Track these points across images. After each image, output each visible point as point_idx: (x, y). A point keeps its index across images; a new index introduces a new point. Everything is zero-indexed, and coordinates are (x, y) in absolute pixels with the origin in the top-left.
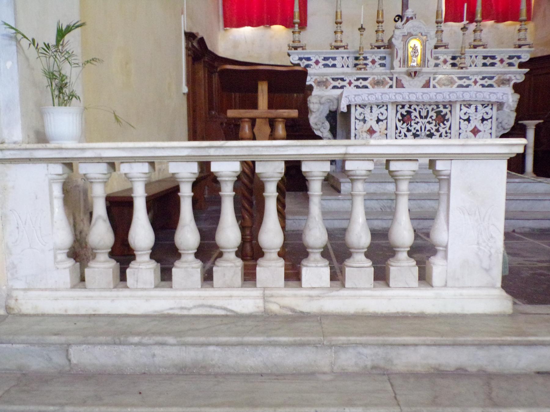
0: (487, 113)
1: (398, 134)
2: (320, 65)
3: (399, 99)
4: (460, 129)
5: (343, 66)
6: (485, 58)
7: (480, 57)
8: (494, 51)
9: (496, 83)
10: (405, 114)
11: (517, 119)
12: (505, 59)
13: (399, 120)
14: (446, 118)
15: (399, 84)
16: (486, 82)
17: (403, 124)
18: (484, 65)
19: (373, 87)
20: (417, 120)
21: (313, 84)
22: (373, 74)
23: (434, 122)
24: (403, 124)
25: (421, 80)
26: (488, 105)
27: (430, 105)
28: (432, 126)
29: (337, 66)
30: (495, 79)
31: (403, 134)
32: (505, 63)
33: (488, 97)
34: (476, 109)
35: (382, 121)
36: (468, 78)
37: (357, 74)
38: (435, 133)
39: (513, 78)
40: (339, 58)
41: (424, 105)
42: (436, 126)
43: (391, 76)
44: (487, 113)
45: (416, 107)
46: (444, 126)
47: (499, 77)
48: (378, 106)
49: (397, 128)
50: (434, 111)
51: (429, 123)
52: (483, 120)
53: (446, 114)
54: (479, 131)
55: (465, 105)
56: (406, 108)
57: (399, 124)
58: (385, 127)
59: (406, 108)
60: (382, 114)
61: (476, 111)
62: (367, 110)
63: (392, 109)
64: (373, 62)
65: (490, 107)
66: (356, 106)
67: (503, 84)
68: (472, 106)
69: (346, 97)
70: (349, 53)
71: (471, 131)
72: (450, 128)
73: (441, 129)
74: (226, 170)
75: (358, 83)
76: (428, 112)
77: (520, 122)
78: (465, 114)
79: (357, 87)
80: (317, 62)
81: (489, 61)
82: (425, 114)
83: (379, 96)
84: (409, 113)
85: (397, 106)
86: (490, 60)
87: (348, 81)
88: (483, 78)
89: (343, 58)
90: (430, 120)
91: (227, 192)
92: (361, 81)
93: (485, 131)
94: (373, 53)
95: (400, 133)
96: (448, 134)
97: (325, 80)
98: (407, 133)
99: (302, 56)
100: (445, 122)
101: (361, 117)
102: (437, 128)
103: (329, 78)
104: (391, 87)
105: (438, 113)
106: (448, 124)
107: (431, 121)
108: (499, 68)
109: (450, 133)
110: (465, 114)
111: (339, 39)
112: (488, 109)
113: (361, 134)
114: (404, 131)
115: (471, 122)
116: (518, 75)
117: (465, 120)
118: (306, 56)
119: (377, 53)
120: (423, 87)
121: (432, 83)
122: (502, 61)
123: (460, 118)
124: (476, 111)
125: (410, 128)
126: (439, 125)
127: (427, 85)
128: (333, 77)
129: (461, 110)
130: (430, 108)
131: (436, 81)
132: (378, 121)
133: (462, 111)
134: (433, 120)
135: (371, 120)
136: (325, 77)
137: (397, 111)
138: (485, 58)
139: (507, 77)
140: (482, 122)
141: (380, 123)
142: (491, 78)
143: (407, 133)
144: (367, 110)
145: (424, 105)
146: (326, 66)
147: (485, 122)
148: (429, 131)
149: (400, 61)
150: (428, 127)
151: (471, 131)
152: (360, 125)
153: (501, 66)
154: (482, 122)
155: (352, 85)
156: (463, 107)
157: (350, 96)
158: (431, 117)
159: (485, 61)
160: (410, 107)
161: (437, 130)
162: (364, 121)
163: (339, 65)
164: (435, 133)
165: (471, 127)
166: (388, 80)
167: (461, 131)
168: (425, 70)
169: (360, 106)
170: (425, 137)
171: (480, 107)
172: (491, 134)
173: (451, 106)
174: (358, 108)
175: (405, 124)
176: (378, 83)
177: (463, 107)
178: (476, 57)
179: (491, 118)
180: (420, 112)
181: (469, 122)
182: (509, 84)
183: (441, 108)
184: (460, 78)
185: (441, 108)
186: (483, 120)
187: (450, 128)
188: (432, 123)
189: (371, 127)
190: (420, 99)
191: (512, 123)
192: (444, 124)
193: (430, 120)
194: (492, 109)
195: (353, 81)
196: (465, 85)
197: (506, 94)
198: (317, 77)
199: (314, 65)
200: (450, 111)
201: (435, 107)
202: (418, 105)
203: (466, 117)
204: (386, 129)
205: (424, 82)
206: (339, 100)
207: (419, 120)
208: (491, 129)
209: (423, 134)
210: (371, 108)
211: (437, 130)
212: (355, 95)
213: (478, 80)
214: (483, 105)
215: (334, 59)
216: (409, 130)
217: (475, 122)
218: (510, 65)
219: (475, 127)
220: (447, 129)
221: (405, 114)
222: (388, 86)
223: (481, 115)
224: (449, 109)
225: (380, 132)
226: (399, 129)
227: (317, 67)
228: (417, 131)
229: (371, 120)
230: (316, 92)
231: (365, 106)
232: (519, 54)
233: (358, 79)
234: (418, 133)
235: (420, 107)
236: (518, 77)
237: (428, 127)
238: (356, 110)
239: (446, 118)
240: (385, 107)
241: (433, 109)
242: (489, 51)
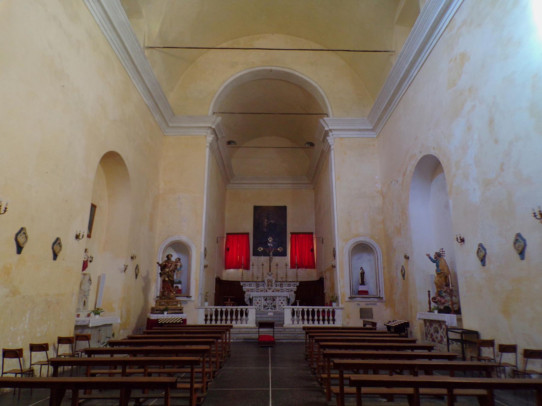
15: (266, 291)
74: (224, 310)
91: (224, 312)
108: (291, 287)
116: (295, 289)
157: (253, 294)
176: (262, 291)
206: (250, 295)
230: (246, 293)
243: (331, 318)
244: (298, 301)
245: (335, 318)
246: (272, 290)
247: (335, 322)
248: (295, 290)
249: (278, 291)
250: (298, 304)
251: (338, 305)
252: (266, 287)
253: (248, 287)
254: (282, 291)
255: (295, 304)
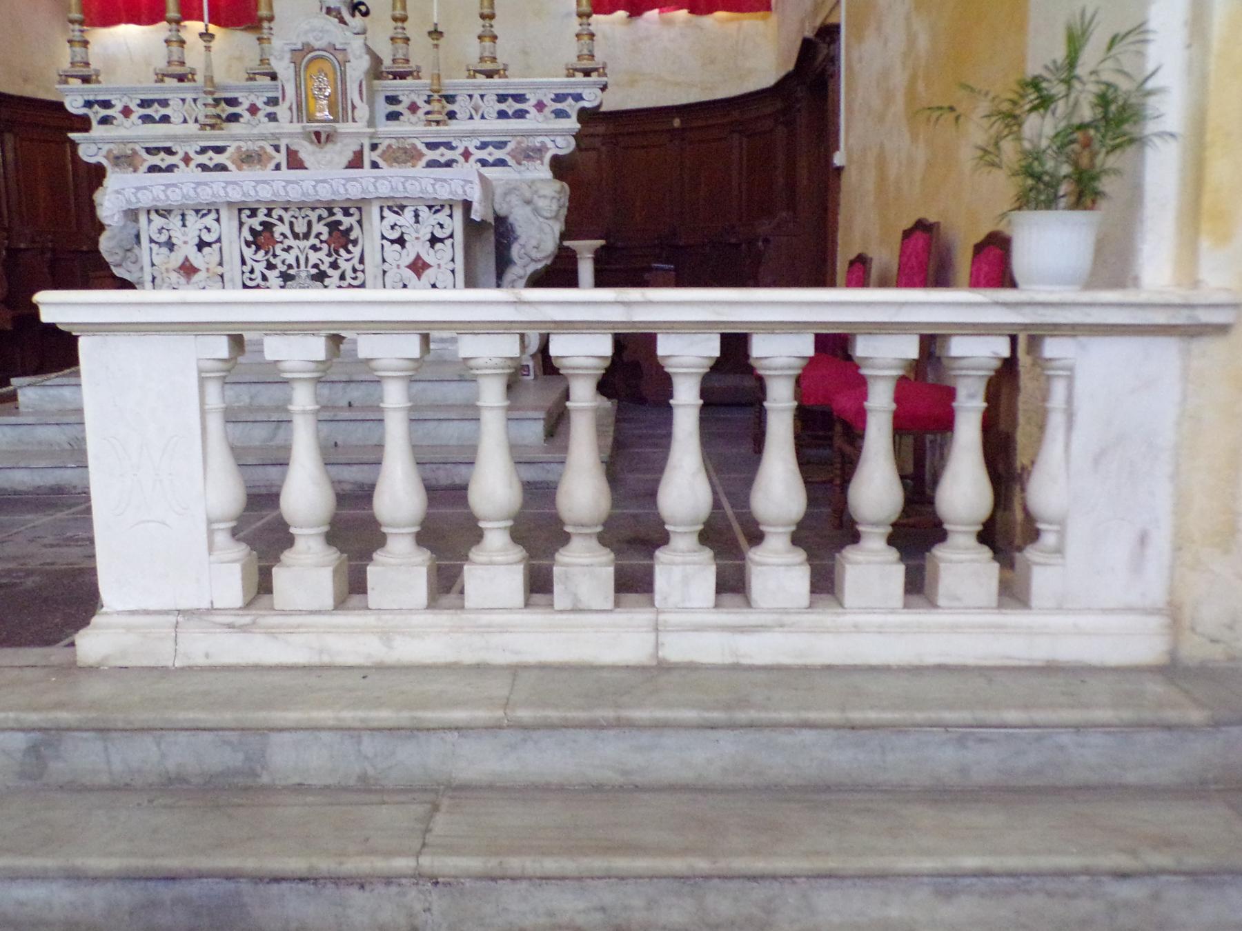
0: (441, 226)
1: (248, 275)
2: (134, 117)
3: (235, 195)
4: (384, 261)
5: (185, 121)
6: (502, 98)
7: (491, 98)
8: (522, 84)
9: (513, 157)
10: (260, 228)
11: (564, 236)
12: (547, 101)
13: (248, 244)
14: (352, 238)
15: (295, 162)
16: (490, 154)
17: (256, 252)
18: (502, 115)
19: (240, 168)
20: (287, 243)
21: (105, 162)
22: (235, 138)
23: (325, 246)
24: (256, 252)
25: (341, 152)
26: (442, 206)
27: (313, 209)
28: (322, 255)
29: (172, 119)
30: (510, 146)
31: (257, 274)
32: (547, 111)
33: (430, 189)
34: (417, 216)
35: (209, 245)
36: (449, 146)
37: (199, 138)
38: (330, 272)
39: (550, 145)
40: (174, 103)
41: (300, 209)
42: (329, 255)
43: (276, 142)
44: (441, 226)
45: (282, 213)
46: (349, 256)
47: (519, 143)
48: (197, 211)
49: (244, 262)
50: (323, 222)
51: (315, 248)
52: (434, 240)
53: (350, 229)
54: (426, 266)
55: (390, 208)
56: (261, 217)
57: (249, 252)
58: (217, 259)
59: (261, 217)
60: (209, 230)
61: (417, 222)
62: (175, 221)
63: (230, 219)
64: (253, 110)
65: (447, 211)
66: (149, 212)
67: (528, 157)
68: (406, 210)
69: (118, 192)
70: (195, 89)
71: (409, 267)
72: (361, 261)
73: (341, 262)
75: (203, 159)
76: (310, 224)
77: (566, 243)
78: (392, 228)
79: (204, 168)
80: (126, 112)
81: (511, 106)
82: (305, 229)
83: (248, 187)
84: (267, 226)
85: (240, 210)
86: (513, 104)
87: (181, 154)
88: (484, 146)
89: (183, 100)
90: (317, 242)
92: (211, 153)
93: (439, 266)
94: (250, 90)
95: (252, 272)
96: (359, 274)
97: (129, 152)
98: (267, 272)
99: (91, 98)
100: (350, 247)
101: (163, 238)
102: (331, 259)
103: (137, 147)
104: (278, 167)
105: (334, 226)
106: (356, 251)
107: (319, 245)
108: (533, 121)
109: (363, 271)
110: (392, 228)
111: (175, 58)
112: (442, 217)
113: (165, 275)
114: (260, 267)
115: (407, 245)
117: (393, 242)
118: (101, 98)
119: (263, 89)
120: (347, 167)
121: (368, 156)
122: (540, 106)
123: (383, 237)
124: (417, 222)
125: (273, 261)
126: (337, 252)
127: (356, 162)
128: (147, 145)
129: (382, 218)
130: (313, 216)
131: (379, 151)
132: (201, 245)
133: (385, 222)
134: (322, 242)
135: (185, 243)
136: (130, 146)
137: (241, 224)
138: (502, 98)
139: (537, 142)
140: (432, 246)
141: (206, 250)
142: (500, 145)
143: (267, 272)
144: (175, 221)
145: (300, 209)
146: (147, 119)
147: (438, 246)
148: (316, 266)
149: (290, 109)
150: (314, 257)
151: (409, 267)
152: (161, 255)
153: (540, 117)
154: (432, 246)
155: (192, 164)
156: (386, 213)
158: (318, 236)
159: (503, 106)
160: (269, 215)
161: (334, 265)
162: (170, 245)
163: (176, 118)
164: (330, 272)
165: (408, 256)
166: (270, 150)
167: (386, 267)
168: (342, 127)
169: (157, 211)
170: (309, 281)
171: (424, 213)
172: (453, 271)
173: (359, 209)
174: (154, 216)
175: (262, 252)
176: (249, 159)
177: (386, 213)
178: (482, 96)
179: (451, 236)
180: (291, 224)
181: (403, 246)
182: (541, 159)
183: (339, 216)
184: (432, 146)
185: (339, 216)
186: (434, 240)
187: (361, 261)
188: (320, 249)
189: (187, 259)
190: (283, 197)
191: (549, 245)
192: (349, 252)
193: (317, 242)
194: (451, 216)
195: (192, 155)
196: (443, 160)
197: (471, 182)
198: (112, 146)
199: (120, 117)
200: (360, 222)
201: (325, 213)
202: (286, 209)
203: (395, 235)
204: (221, 264)
205: (349, 155)
207: (291, 241)
208: (453, 260)
209: (304, 274)
210: (183, 215)
211: (334, 265)
212: (138, 189)
213: (472, 149)
214: (430, 207)
215: (164, 103)
216: (270, 266)
217: (417, 247)
218: (560, 114)
219: (418, 257)
220: (356, 261)
221: (260, 228)
222: (272, 165)
223: (429, 229)
224: (356, 217)
225: (208, 270)
226: (249, 262)
227: (127, 123)
228: (290, 266)
229: (185, 243)
231: (169, 211)
232: (579, 91)
233: (203, 150)
234: (291, 272)
235: (291, 213)
236: (560, 141)
237: (314, 257)
238: (150, 221)
239: (352, 238)
240: (213, 215)
241: (320, 218)
242: (508, 84)
243: (964, 489)
244: (586, 250)
245: (1046, 491)
246: (341, 152)
247: (1044, 577)
248: (565, 146)
249: (407, 155)
250: (586, 269)
251: (1113, 263)
252: (288, 126)
253: (131, 130)
254: (440, 155)
255: (558, 273)
